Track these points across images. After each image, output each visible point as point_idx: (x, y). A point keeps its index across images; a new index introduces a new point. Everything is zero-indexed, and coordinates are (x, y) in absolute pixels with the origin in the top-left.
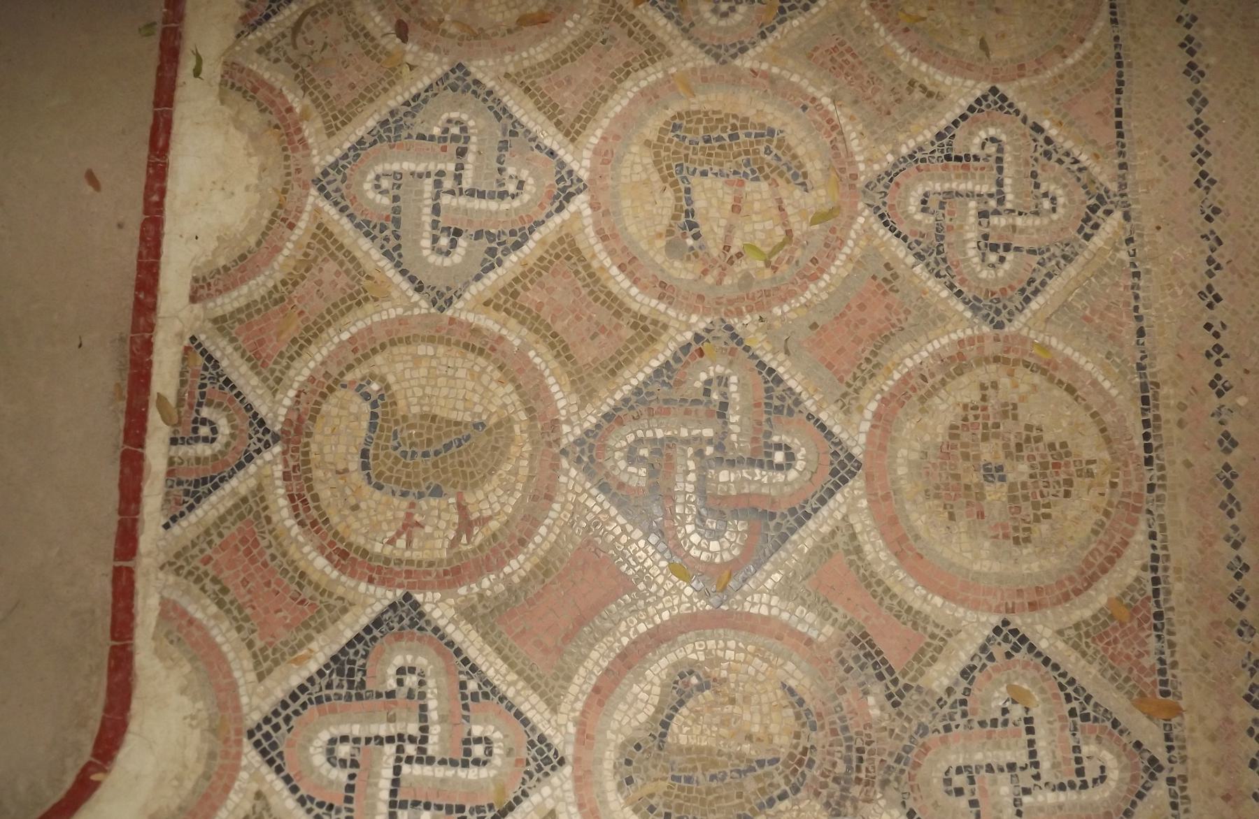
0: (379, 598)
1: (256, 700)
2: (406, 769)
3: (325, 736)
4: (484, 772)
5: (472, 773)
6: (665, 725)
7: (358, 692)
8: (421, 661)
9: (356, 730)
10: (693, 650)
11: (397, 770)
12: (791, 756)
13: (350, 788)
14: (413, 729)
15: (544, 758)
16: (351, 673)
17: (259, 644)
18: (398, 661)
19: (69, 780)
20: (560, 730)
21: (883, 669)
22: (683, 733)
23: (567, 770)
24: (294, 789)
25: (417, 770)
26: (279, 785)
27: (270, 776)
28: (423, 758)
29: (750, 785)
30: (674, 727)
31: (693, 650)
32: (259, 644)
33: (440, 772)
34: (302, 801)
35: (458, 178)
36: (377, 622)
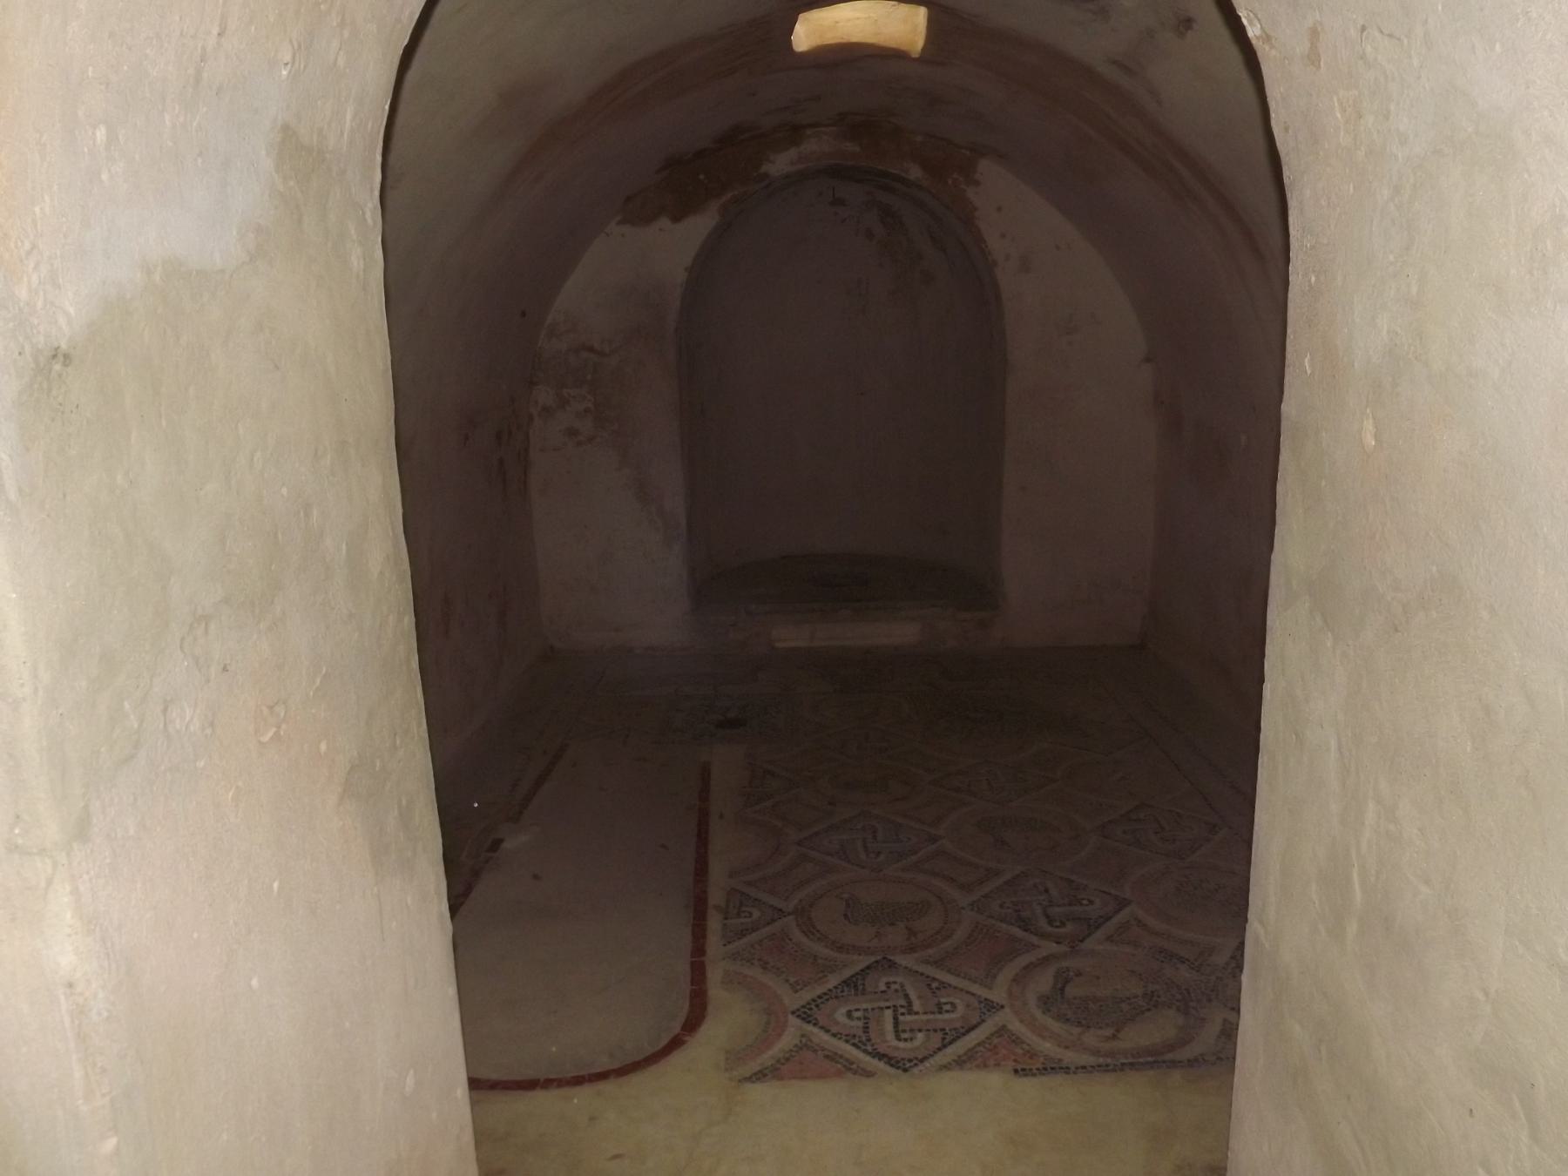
0: (864, 961)
1: (792, 1000)
2: (901, 1018)
3: (843, 1010)
4: (953, 1016)
5: (947, 1016)
6: (1062, 989)
7: (864, 992)
8: (899, 980)
9: (865, 1006)
10: (1065, 964)
11: (896, 1019)
12: (1145, 994)
13: (866, 1029)
14: (903, 1002)
15: (991, 1007)
16: (856, 986)
17: (792, 980)
18: (885, 980)
19: (664, 1042)
20: (998, 995)
21: (1182, 960)
22: (1071, 991)
23: (1007, 1010)
24: (828, 1031)
25: (909, 1018)
26: (815, 1030)
27: (810, 1028)
28: (910, 1012)
29: (1125, 1006)
30: (1068, 989)
31: (1065, 964)
32: (792, 980)
33: (925, 1017)
34: (834, 1035)
35: (875, 837)
36: (868, 967)
